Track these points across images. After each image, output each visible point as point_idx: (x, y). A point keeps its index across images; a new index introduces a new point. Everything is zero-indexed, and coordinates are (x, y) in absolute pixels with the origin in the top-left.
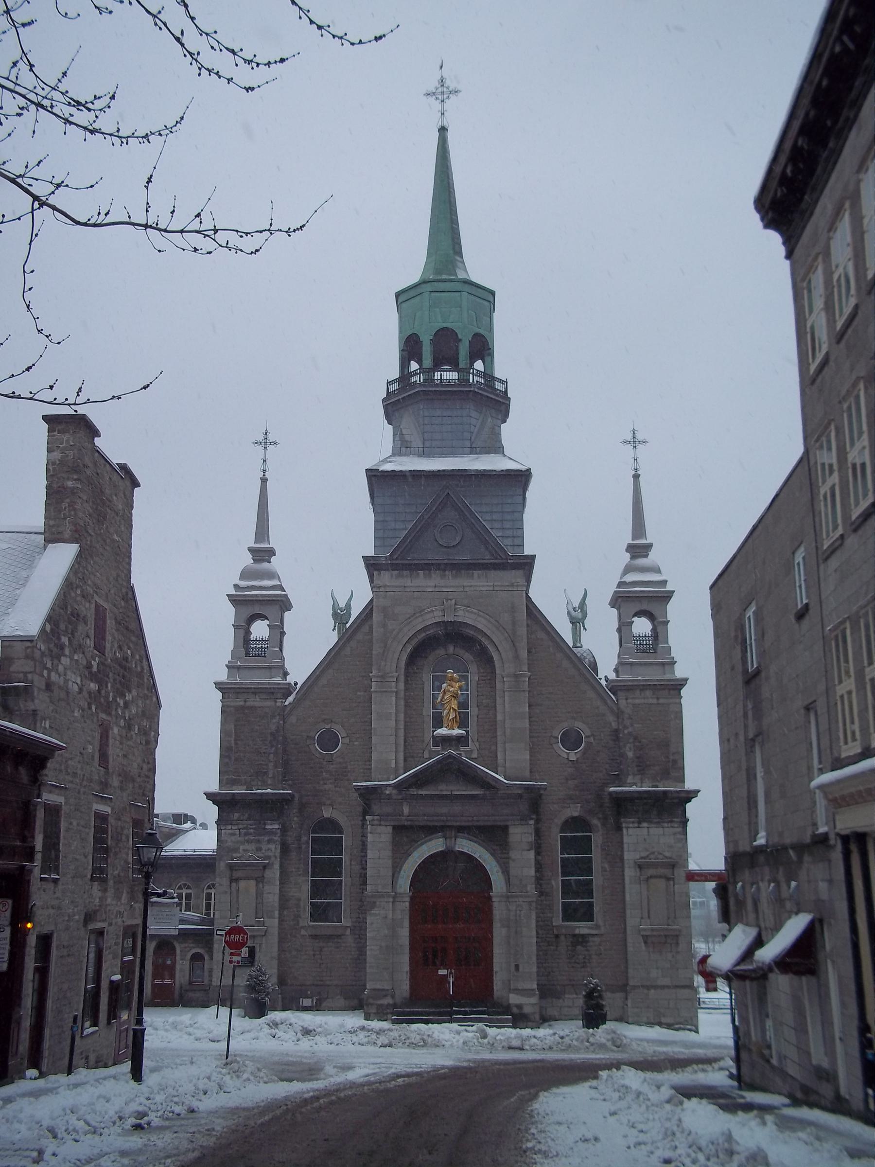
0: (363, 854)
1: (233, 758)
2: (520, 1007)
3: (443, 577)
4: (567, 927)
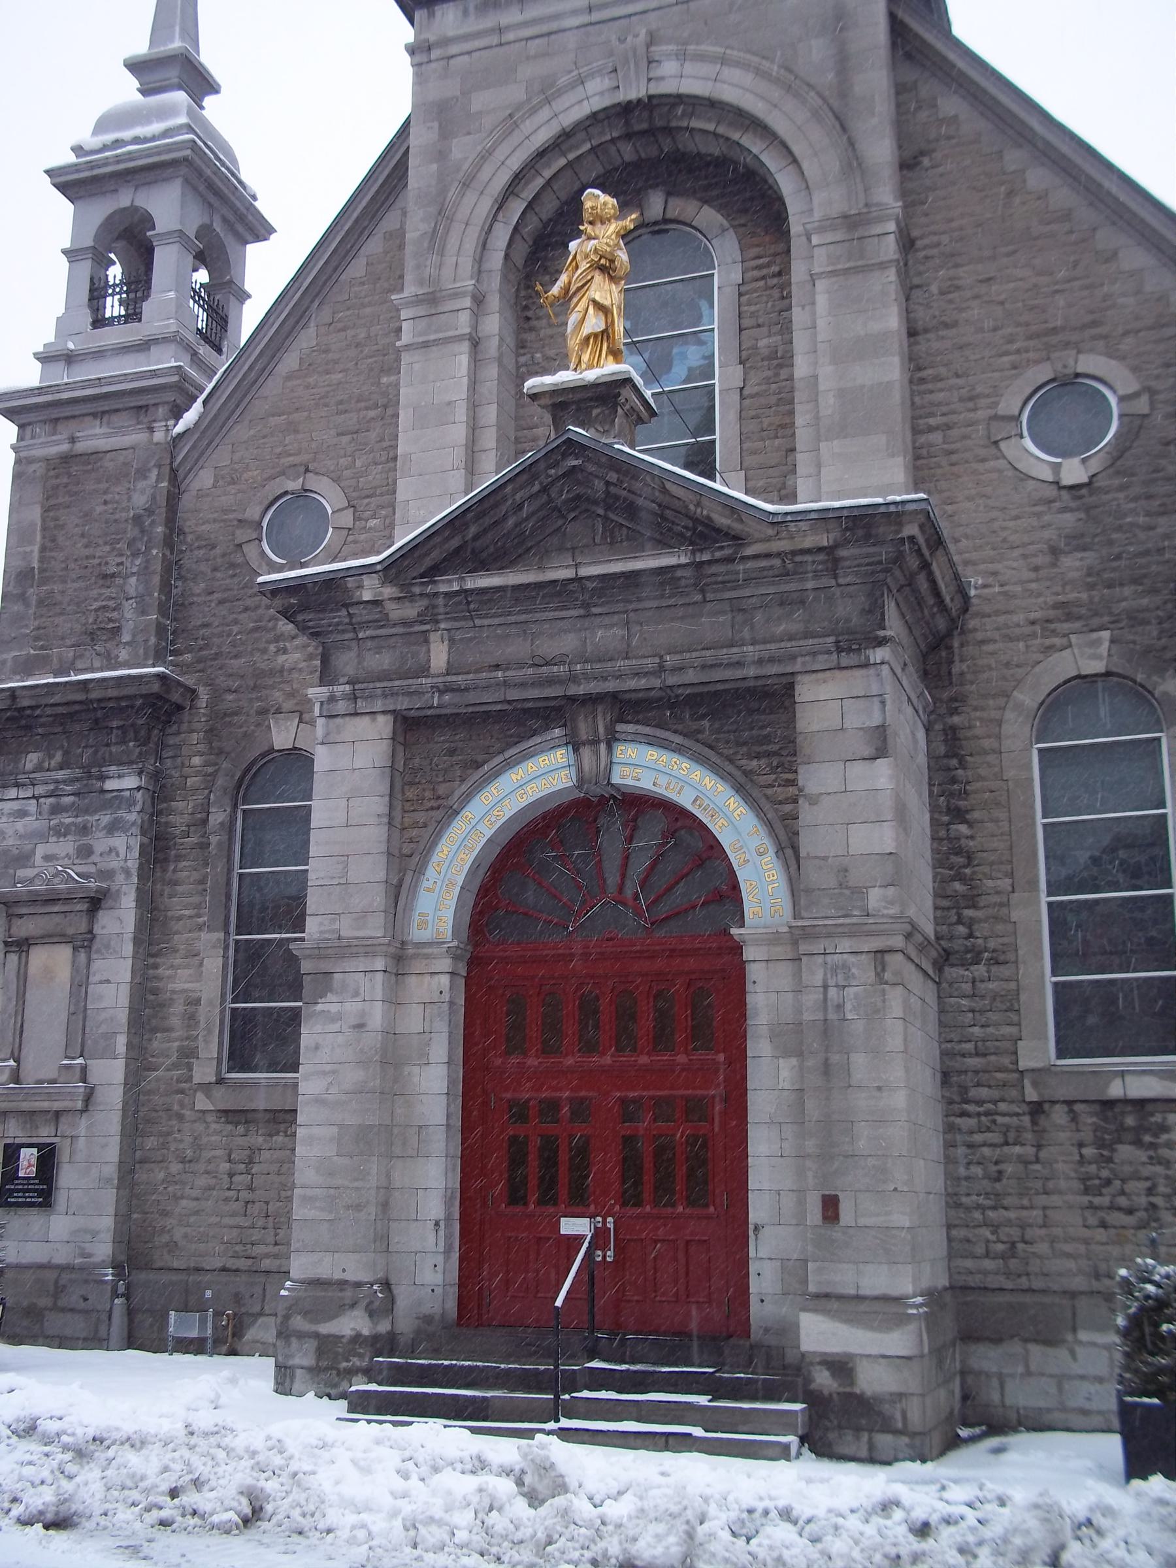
1: (34, 601)
2: (841, 1366)
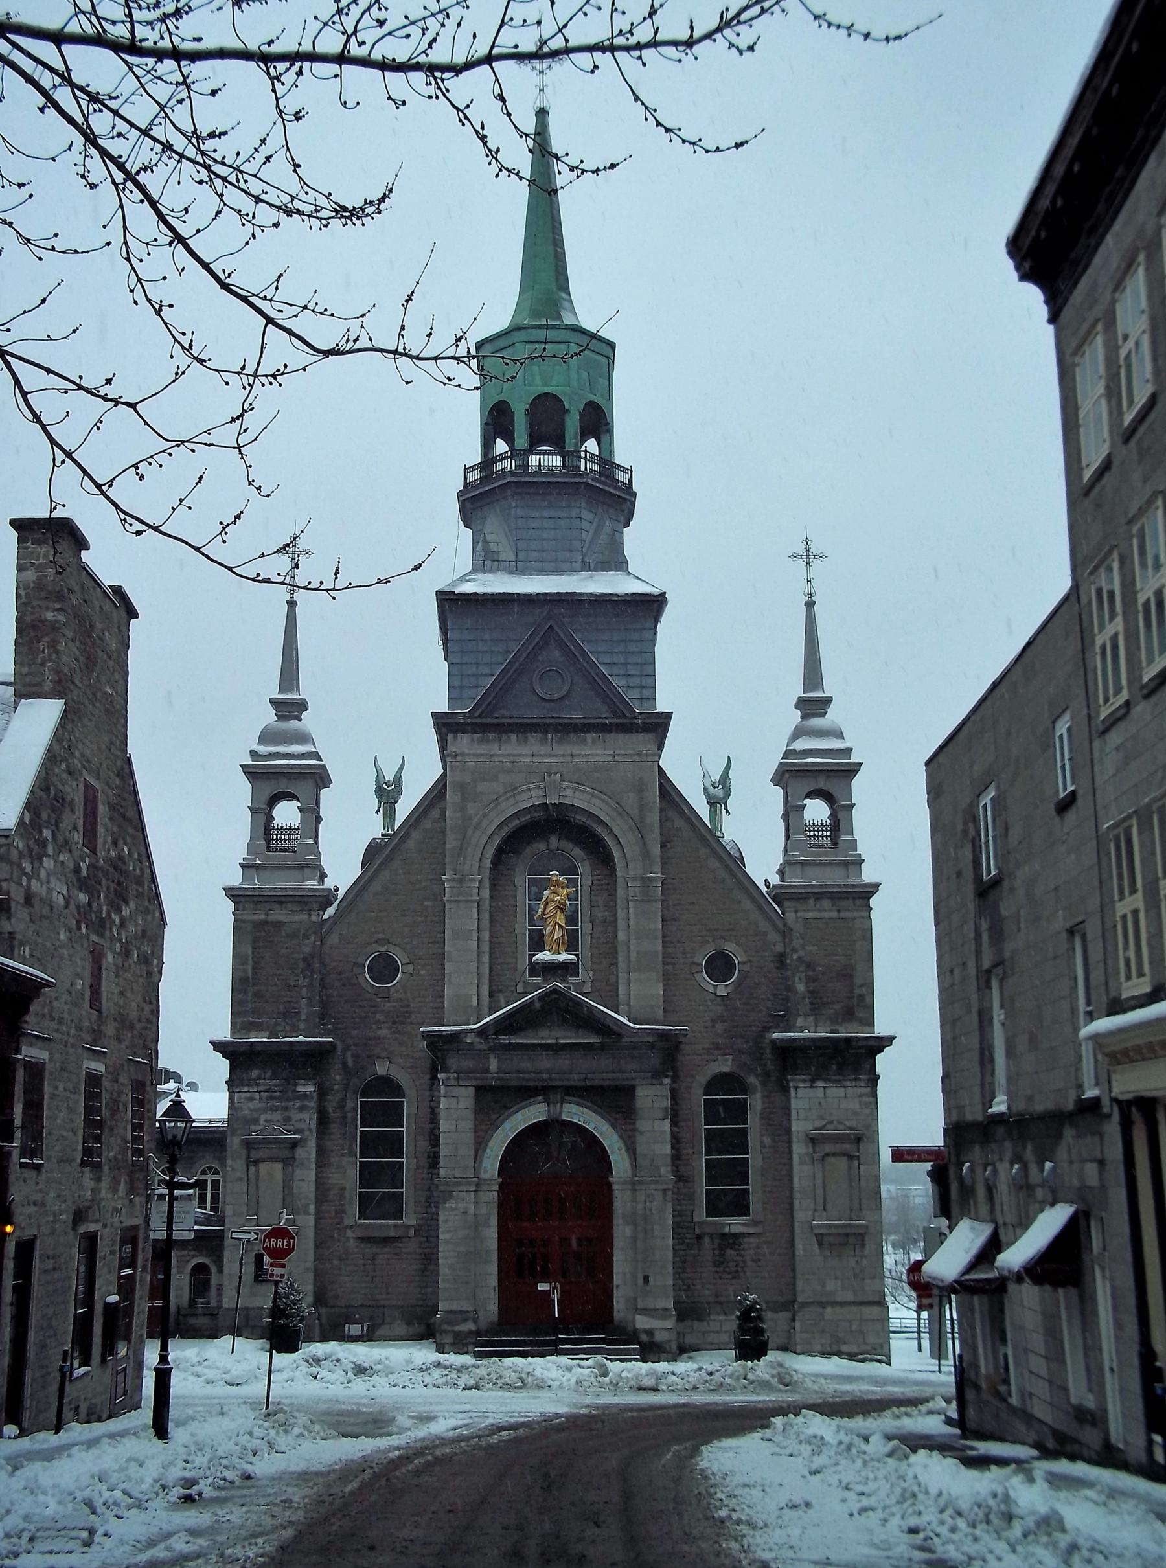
2: (650, 1332)
3: (544, 741)
4: (713, 1223)
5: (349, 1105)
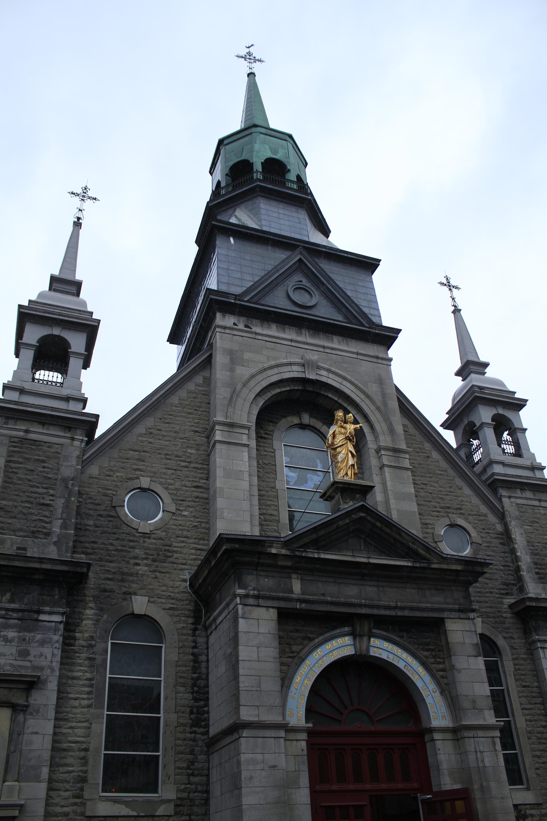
0: (195, 675)
5: (99, 647)
